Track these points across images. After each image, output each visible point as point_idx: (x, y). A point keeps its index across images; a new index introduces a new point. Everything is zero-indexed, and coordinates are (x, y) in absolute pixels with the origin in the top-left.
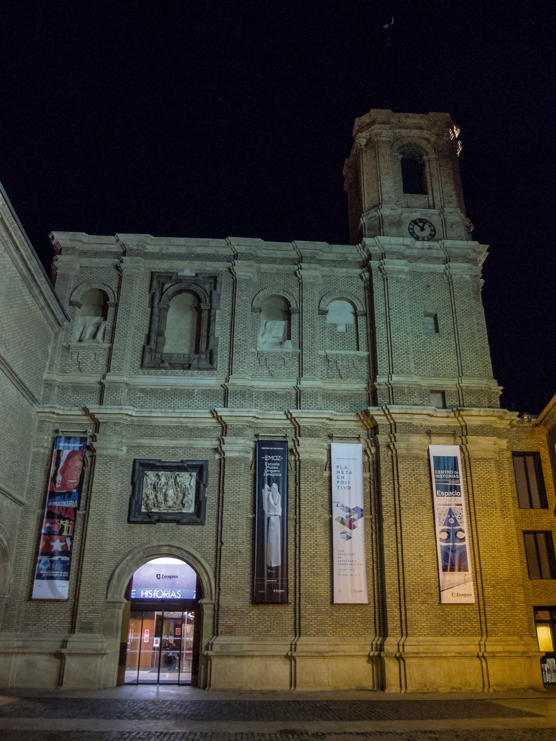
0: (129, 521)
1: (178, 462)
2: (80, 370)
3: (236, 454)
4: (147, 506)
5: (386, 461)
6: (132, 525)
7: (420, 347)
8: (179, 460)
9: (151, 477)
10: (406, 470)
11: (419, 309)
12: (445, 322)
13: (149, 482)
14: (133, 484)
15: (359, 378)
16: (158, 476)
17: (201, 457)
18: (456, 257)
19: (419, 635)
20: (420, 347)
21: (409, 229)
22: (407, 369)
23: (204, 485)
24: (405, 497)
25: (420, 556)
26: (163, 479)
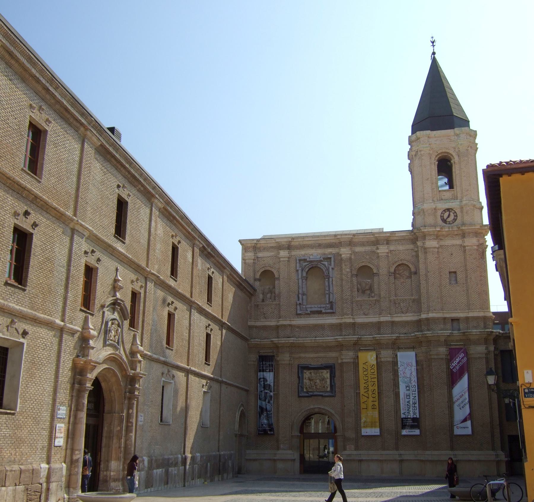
0: (299, 397)
1: (320, 365)
2: (265, 318)
3: (349, 360)
4: (306, 388)
5: (426, 361)
6: (300, 398)
7: (446, 293)
8: (320, 364)
9: (307, 374)
10: (436, 366)
11: (446, 269)
12: (460, 276)
13: (307, 376)
14: (299, 377)
15: (413, 312)
16: (311, 373)
17: (331, 362)
18: (469, 233)
19: (442, 450)
20: (446, 293)
21: (442, 213)
22: (438, 308)
23: (333, 376)
24: (436, 381)
25: (443, 411)
26: (313, 374)
